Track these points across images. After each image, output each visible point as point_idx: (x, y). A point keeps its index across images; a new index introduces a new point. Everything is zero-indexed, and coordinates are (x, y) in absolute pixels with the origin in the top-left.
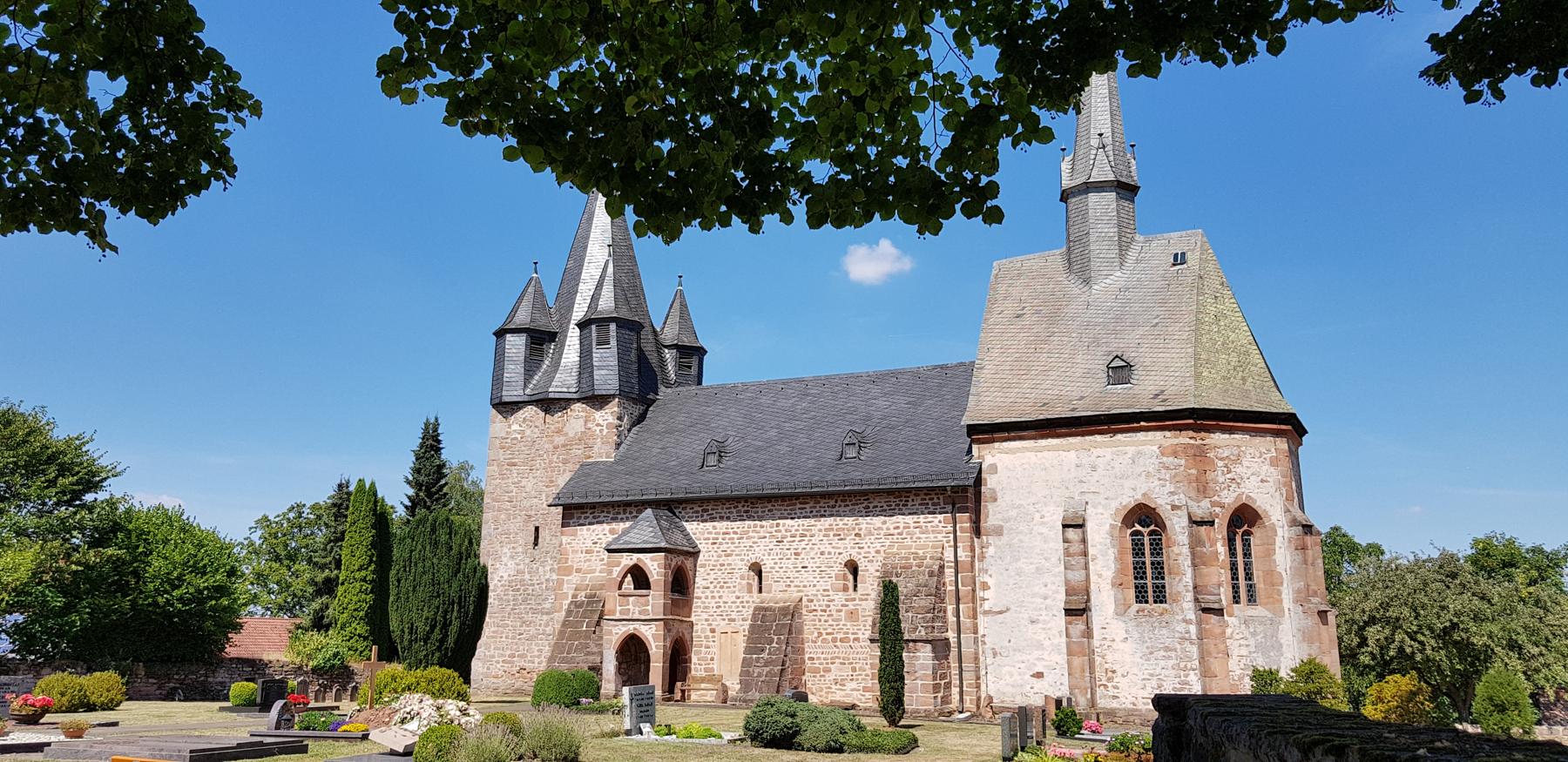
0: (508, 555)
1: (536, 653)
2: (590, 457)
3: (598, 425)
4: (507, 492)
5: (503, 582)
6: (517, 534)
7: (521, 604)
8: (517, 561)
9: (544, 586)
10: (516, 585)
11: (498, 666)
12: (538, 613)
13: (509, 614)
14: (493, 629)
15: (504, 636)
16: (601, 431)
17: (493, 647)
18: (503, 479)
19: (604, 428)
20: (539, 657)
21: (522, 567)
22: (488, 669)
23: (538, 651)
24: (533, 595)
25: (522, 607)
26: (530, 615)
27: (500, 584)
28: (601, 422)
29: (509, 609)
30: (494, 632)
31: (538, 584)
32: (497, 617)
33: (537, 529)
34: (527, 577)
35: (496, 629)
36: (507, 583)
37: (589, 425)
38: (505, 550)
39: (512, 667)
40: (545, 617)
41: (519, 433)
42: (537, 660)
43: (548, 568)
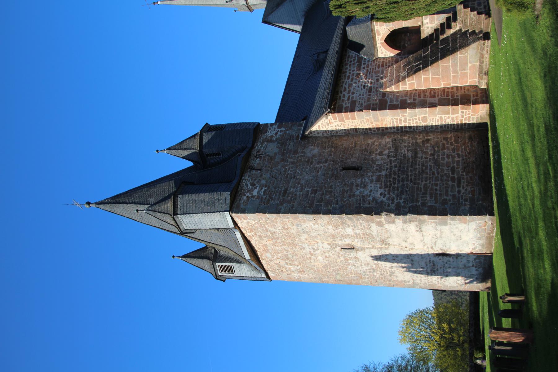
0: (362, 190)
1: (450, 160)
2: (298, 136)
3: (276, 134)
4: (308, 195)
5: (386, 193)
6: (345, 184)
7: (407, 175)
8: (369, 182)
9: (393, 159)
10: (390, 181)
11: (463, 191)
12: (416, 161)
13: (415, 184)
14: (428, 198)
15: (435, 187)
16: (281, 131)
17: (445, 197)
18: (296, 199)
19: (280, 130)
20: (453, 157)
21: (374, 178)
22: (466, 200)
23: (448, 158)
24: (400, 166)
25: (409, 174)
26: (418, 167)
27: (387, 196)
28: (275, 132)
29: (411, 185)
30: (431, 197)
31: (391, 164)
32: (418, 195)
33: (344, 169)
34: (383, 173)
35: (428, 196)
36: (387, 189)
37: (274, 139)
38: (358, 193)
39: (463, 179)
40: (420, 155)
41: (262, 189)
42: (456, 159)
43: (378, 157)
